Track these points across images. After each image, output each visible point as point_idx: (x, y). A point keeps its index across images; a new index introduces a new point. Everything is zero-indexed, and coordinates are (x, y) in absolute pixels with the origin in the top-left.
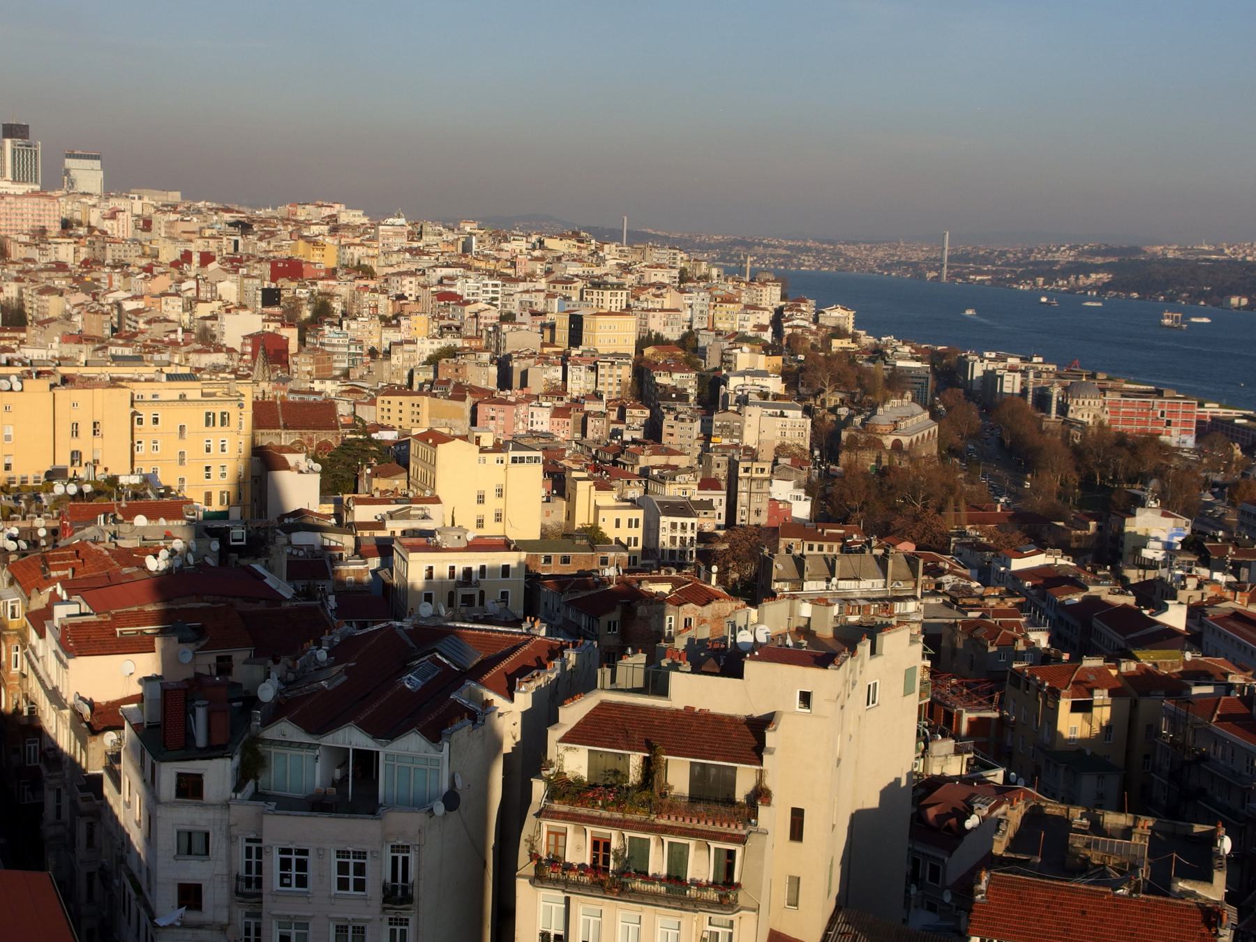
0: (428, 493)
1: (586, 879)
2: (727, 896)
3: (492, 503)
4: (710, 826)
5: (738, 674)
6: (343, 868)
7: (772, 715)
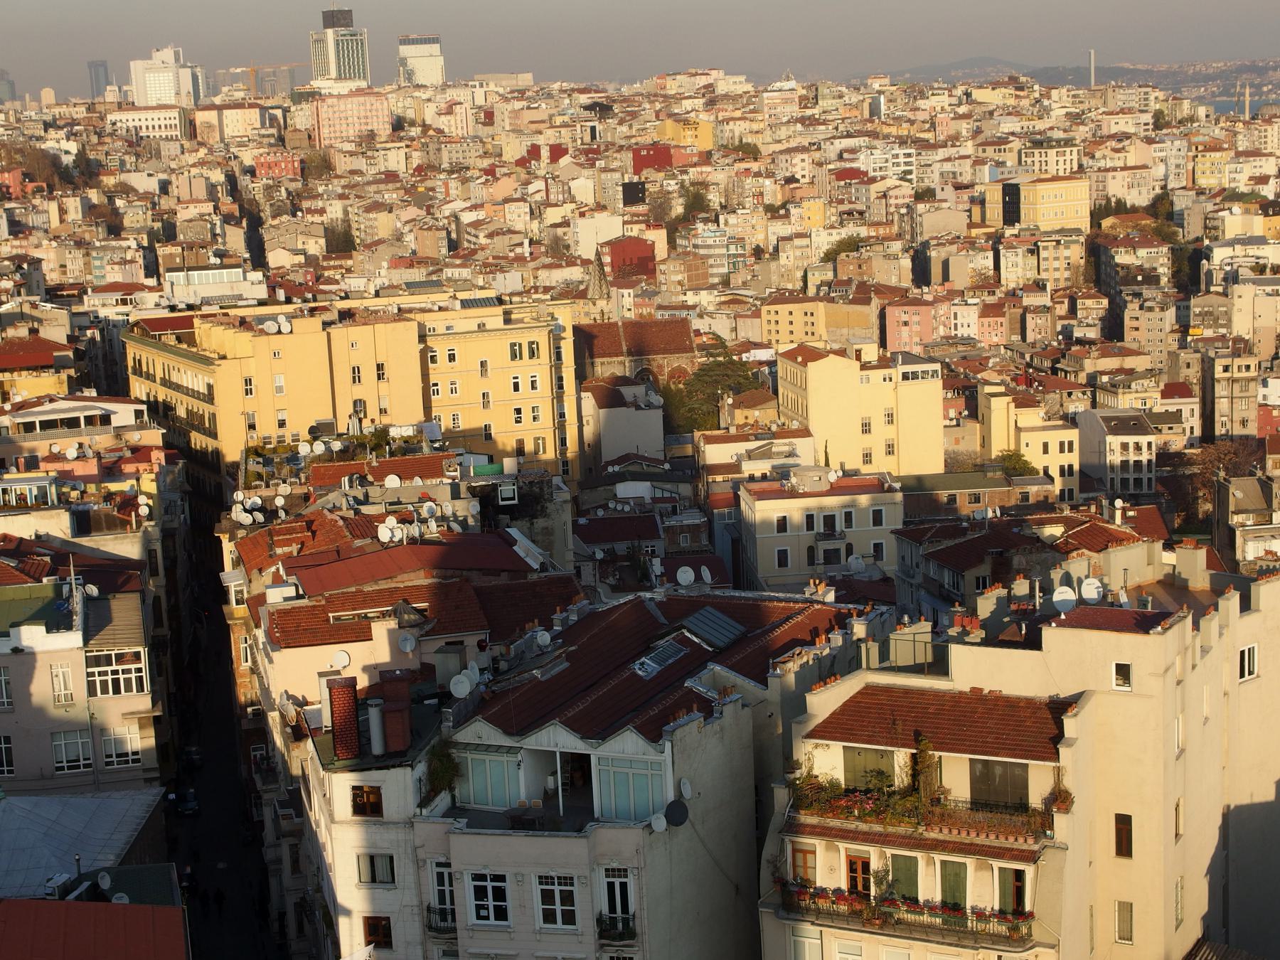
0: (795, 425)
1: (843, 908)
2: (1015, 929)
3: (881, 432)
4: (992, 841)
5: (1033, 642)
6: (547, 897)
7: (1083, 692)
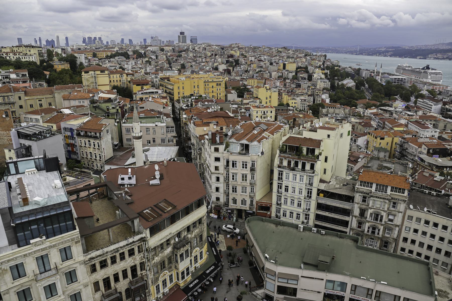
3: (269, 99)
6: (243, 165)
